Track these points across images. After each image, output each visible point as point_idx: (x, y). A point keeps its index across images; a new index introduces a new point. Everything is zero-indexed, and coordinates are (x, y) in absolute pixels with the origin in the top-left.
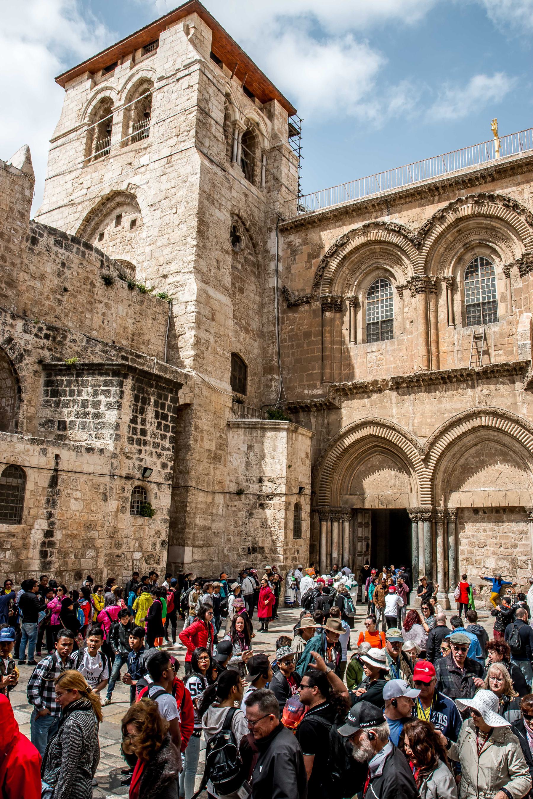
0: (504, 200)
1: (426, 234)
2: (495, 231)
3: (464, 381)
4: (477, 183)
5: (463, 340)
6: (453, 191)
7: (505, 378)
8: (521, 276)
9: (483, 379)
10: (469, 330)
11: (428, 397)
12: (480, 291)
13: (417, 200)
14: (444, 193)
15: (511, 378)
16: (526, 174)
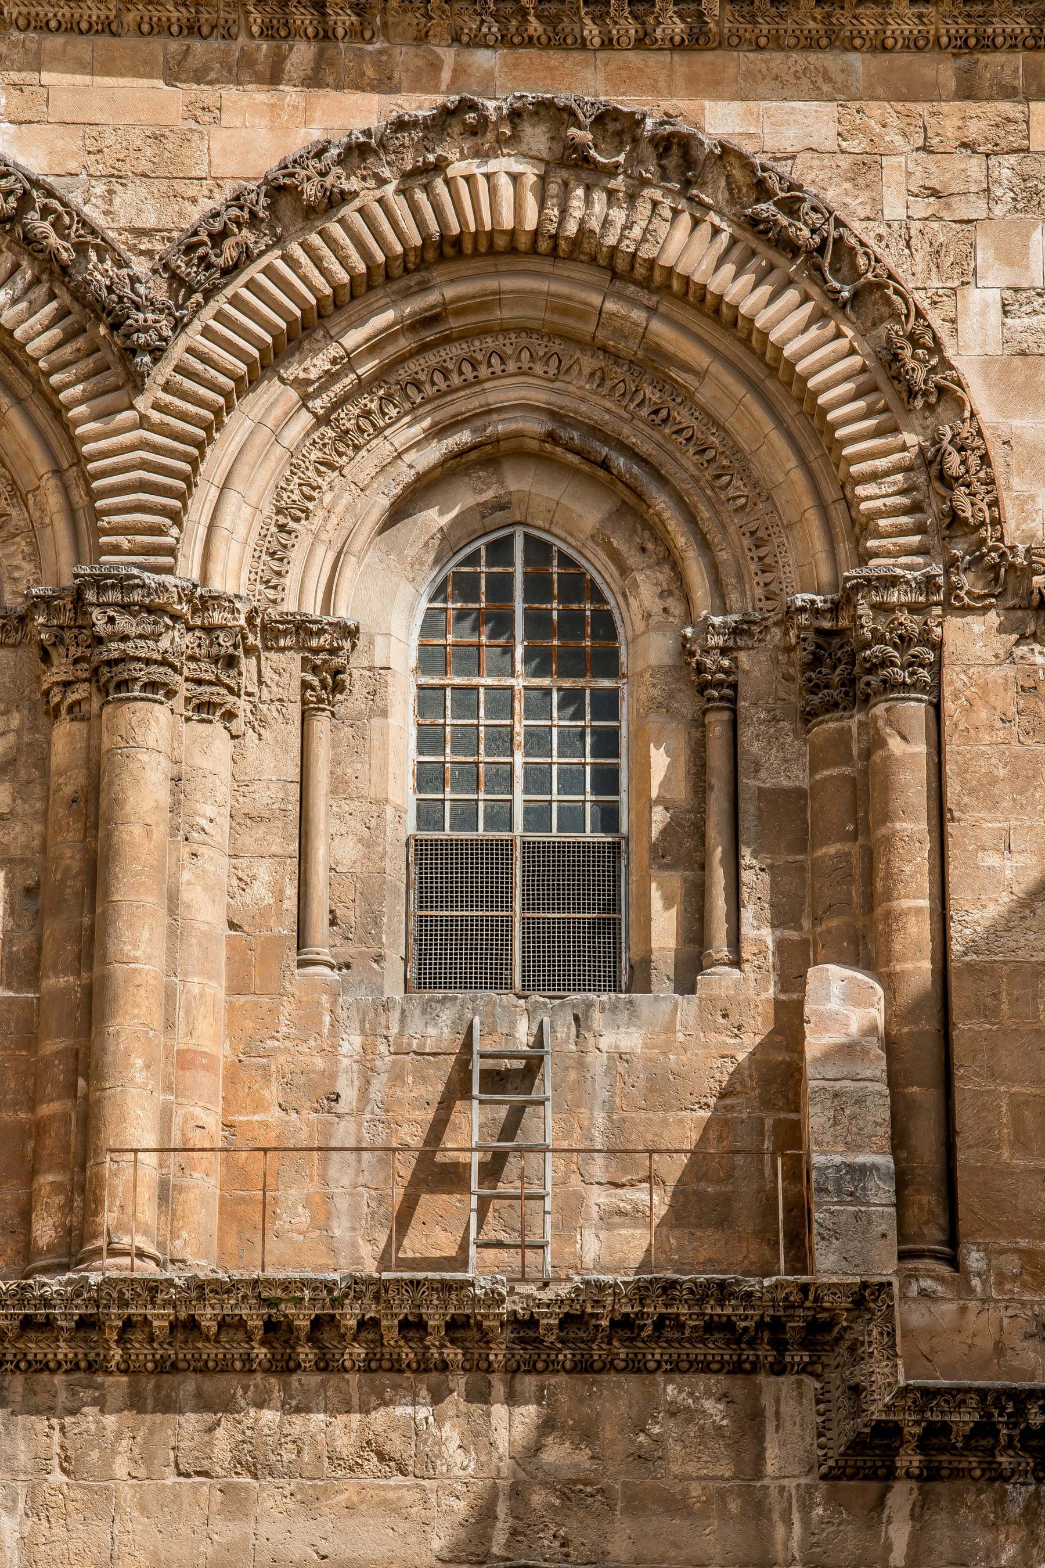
0: (762, 190)
1: (209, 294)
2: (663, 382)
3: (423, 1367)
4: (591, 30)
5: (397, 1077)
6: (422, 38)
7: (702, 1382)
8: (808, 717)
9: (552, 1367)
10: (447, 1015)
11: (147, 1458)
12: (519, 759)
13: (160, 29)
14: (356, 34)
15: (737, 1386)
16: (904, 58)
